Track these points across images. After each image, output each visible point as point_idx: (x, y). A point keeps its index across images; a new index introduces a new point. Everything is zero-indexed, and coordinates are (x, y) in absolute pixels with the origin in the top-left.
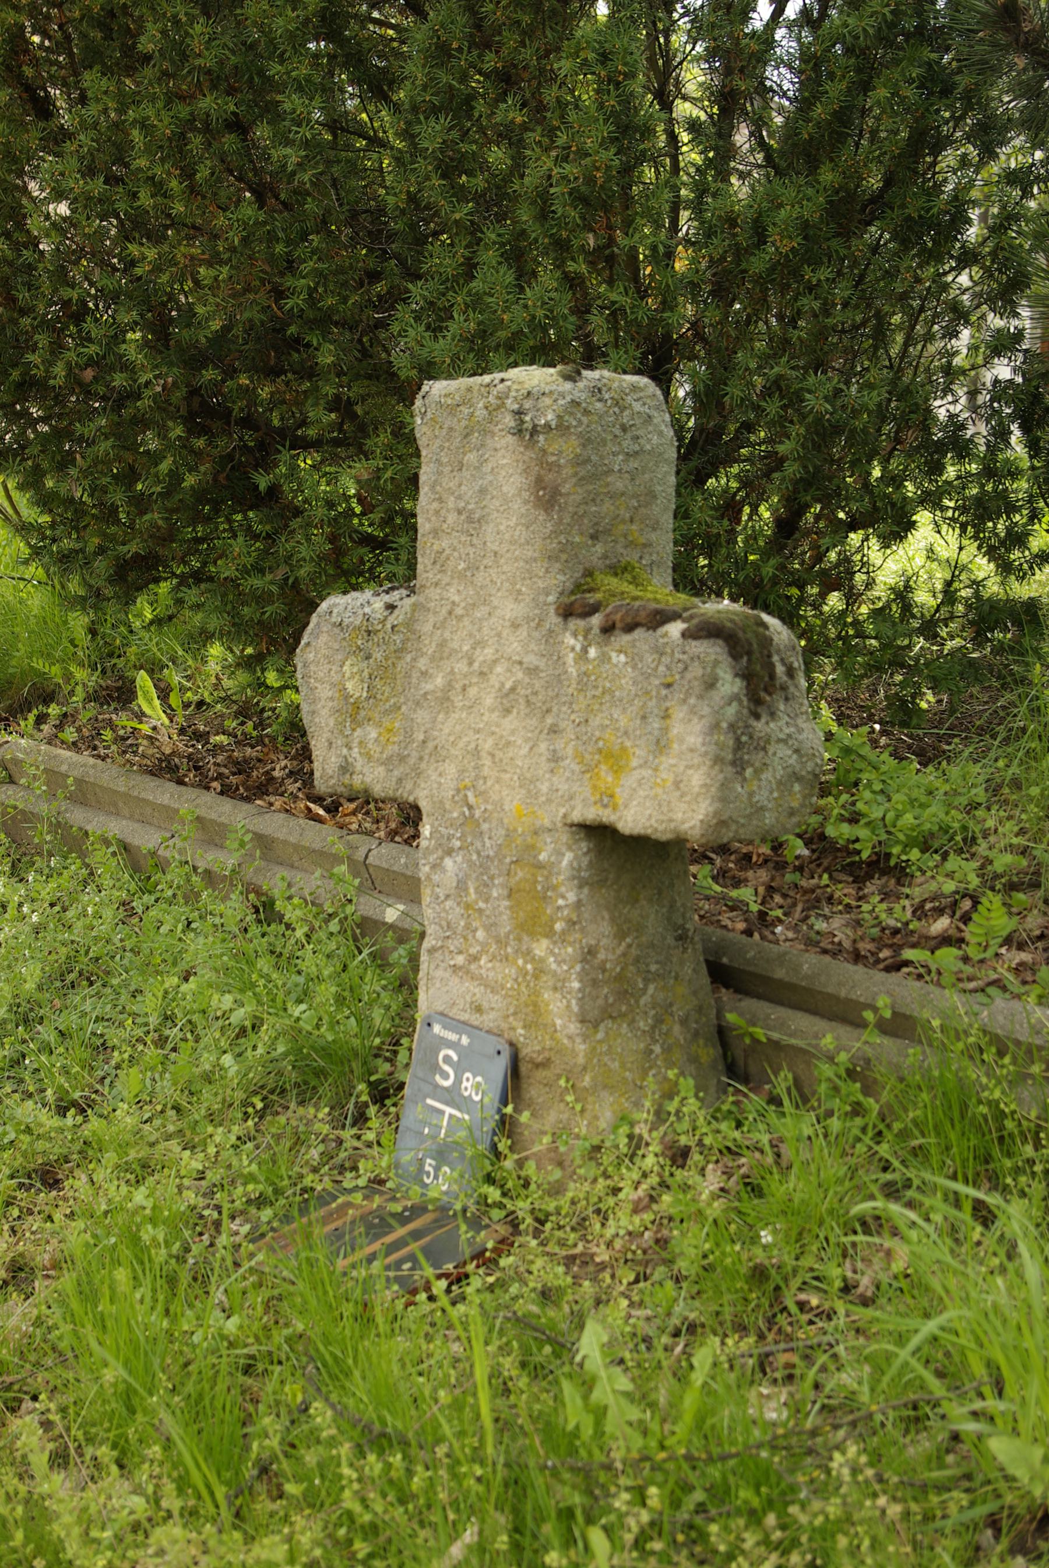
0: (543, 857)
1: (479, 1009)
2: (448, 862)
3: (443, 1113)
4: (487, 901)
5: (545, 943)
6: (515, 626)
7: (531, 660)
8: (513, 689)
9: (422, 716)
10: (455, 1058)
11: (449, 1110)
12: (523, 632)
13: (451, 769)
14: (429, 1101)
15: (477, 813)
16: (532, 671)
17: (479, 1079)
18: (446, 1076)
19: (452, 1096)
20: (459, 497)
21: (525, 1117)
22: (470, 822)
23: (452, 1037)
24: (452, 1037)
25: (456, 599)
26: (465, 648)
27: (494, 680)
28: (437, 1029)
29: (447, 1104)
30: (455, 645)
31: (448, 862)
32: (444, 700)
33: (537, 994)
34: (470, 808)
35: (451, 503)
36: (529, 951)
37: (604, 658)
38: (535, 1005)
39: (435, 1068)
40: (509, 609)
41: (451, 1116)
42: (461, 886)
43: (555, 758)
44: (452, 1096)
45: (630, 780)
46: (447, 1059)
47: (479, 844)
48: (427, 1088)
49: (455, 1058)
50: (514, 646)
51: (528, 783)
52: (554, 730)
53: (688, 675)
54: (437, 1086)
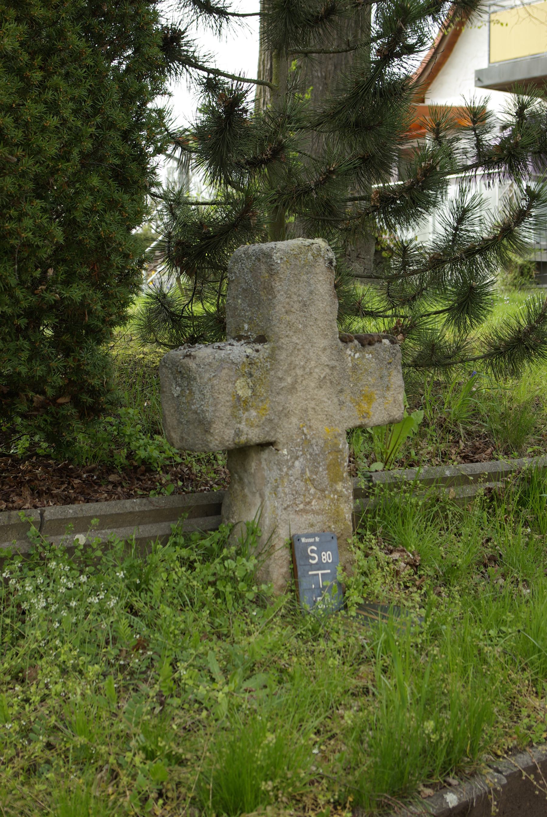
0: (341, 447)
1: (312, 525)
2: (297, 463)
3: (318, 575)
4: (316, 474)
5: (340, 484)
6: (325, 349)
7: (333, 363)
8: (325, 377)
9: (281, 398)
10: (315, 548)
11: (320, 572)
12: (328, 352)
13: (294, 420)
14: (310, 573)
15: (308, 437)
16: (333, 368)
17: (329, 552)
18: (314, 558)
19: (320, 566)
20: (299, 295)
21: (263, 587)
22: (307, 442)
23: (311, 540)
24: (311, 540)
25: (297, 341)
26: (302, 363)
27: (314, 375)
28: (303, 540)
29: (319, 570)
30: (297, 363)
31: (297, 463)
32: (292, 389)
33: (338, 507)
34: (305, 435)
35: (295, 298)
36: (336, 490)
37: (363, 357)
38: (338, 512)
39: (309, 557)
40: (323, 343)
41: (322, 574)
42: (303, 473)
43: (341, 404)
44: (320, 566)
45: (375, 405)
46: (312, 551)
47: (311, 450)
48: (307, 568)
49: (315, 548)
50: (324, 359)
51: (329, 417)
52: (341, 391)
53: (397, 358)
54: (311, 564)
